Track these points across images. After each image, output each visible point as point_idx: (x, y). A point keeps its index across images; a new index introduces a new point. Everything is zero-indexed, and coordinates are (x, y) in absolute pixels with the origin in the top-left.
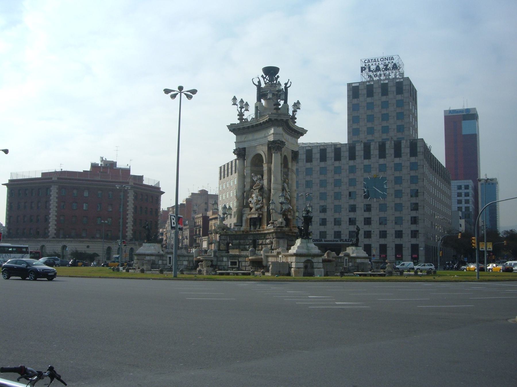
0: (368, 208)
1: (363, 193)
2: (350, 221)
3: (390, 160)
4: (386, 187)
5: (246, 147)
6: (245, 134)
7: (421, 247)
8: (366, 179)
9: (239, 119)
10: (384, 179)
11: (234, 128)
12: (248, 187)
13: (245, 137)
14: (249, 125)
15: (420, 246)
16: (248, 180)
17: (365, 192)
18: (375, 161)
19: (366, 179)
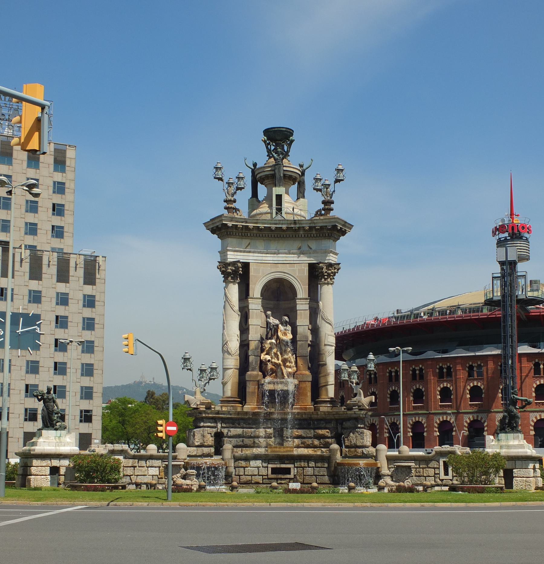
4: (40, 331)
9: (226, 208)
10: (37, 317)
13: (249, 243)
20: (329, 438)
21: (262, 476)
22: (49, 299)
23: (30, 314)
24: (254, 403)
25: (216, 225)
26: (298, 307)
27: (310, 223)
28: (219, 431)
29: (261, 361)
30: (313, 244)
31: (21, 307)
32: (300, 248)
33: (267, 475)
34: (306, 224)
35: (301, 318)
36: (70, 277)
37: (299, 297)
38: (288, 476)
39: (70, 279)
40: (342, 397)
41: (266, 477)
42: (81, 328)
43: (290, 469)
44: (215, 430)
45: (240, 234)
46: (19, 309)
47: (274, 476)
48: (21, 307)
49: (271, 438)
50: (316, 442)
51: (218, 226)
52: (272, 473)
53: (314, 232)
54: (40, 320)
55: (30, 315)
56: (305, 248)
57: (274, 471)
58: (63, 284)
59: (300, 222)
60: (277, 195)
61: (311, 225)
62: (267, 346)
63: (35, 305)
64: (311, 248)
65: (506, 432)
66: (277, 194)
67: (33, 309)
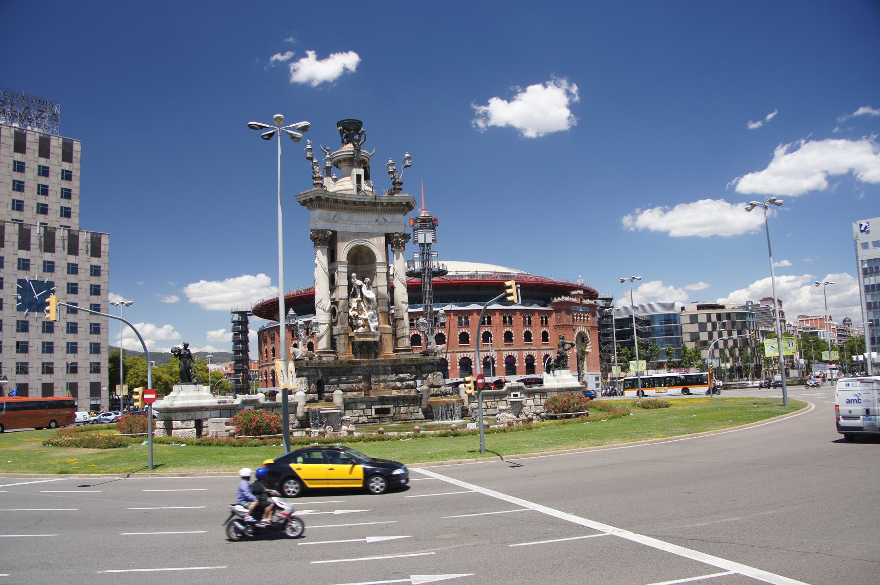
0: (23, 327)
1: (16, 302)
2: (18, 347)
3: (61, 257)
5: (337, 230)
6: (335, 211)
7: (104, 387)
8: (20, 282)
10: (51, 284)
11: (327, 196)
12: (342, 293)
14: (354, 200)
15: (102, 385)
16: (342, 281)
17: (18, 301)
18: (36, 256)
19: (20, 282)
20: (409, 380)
21: (368, 416)
22: (61, 269)
23: (44, 281)
24: (350, 353)
25: (309, 198)
26: (378, 270)
27: (388, 200)
28: (320, 379)
29: (350, 317)
30: (388, 217)
31: (37, 275)
32: (377, 221)
33: (372, 415)
34: (385, 200)
35: (381, 279)
36: (79, 250)
37: (378, 261)
38: (388, 415)
39: (79, 252)
40: (273, 348)
41: (371, 417)
42: (89, 294)
43: (389, 409)
44: (317, 379)
45: (329, 207)
46: (35, 277)
47: (376, 416)
48: (37, 275)
49: (361, 383)
50: (399, 384)
51: (312, 198)
52: (376, 413)
53: (390, 207)
54: (54, 287)
55: (45, 282)
56: (381, 220)
57: (377, 411)
58: (73, 257)
59: (379, 198)
60: (357, 175)
61: (389, 201)
62: (354, 305)
63: (49, 274)
64: (386, 221)
65: (560, 369)
66: (358, 174)
67: (47, 278)
